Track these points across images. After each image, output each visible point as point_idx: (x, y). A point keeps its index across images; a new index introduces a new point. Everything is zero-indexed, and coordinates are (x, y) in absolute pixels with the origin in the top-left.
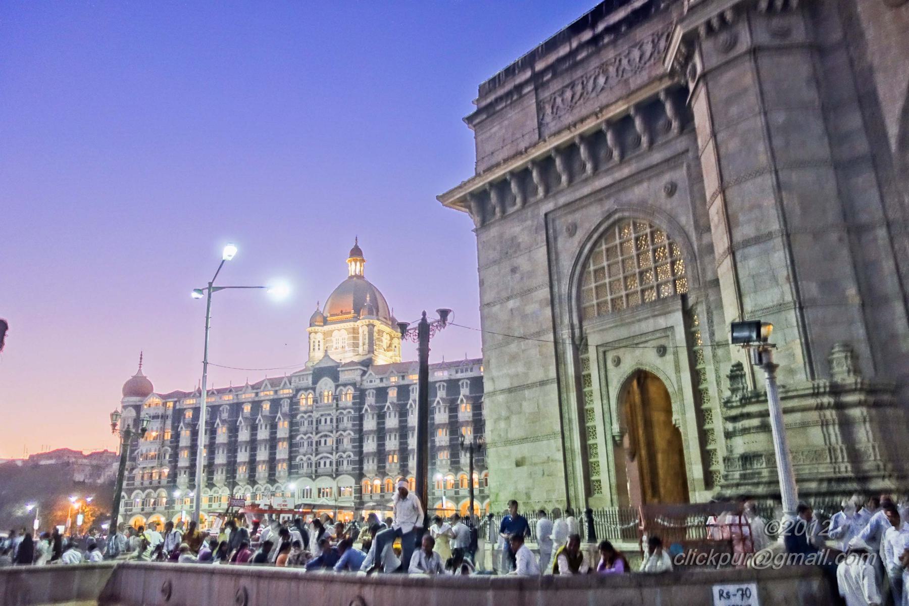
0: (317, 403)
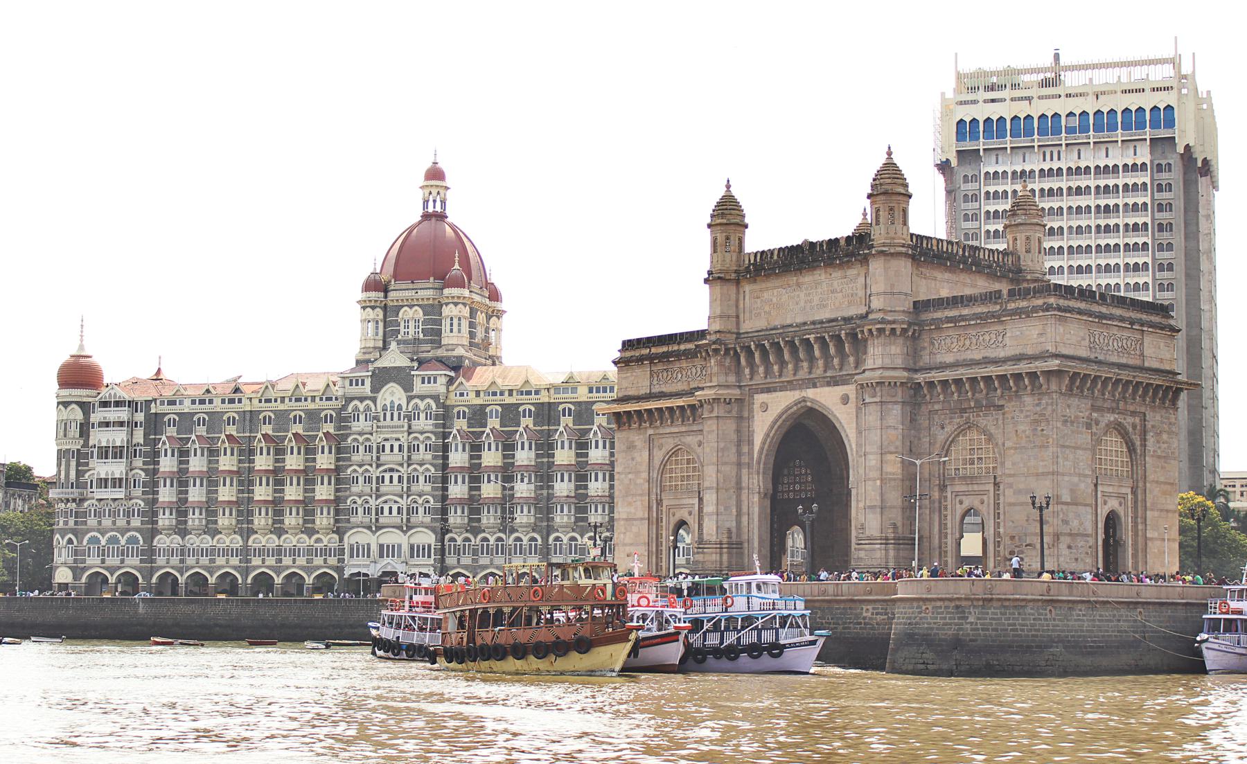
0: (379, 421)
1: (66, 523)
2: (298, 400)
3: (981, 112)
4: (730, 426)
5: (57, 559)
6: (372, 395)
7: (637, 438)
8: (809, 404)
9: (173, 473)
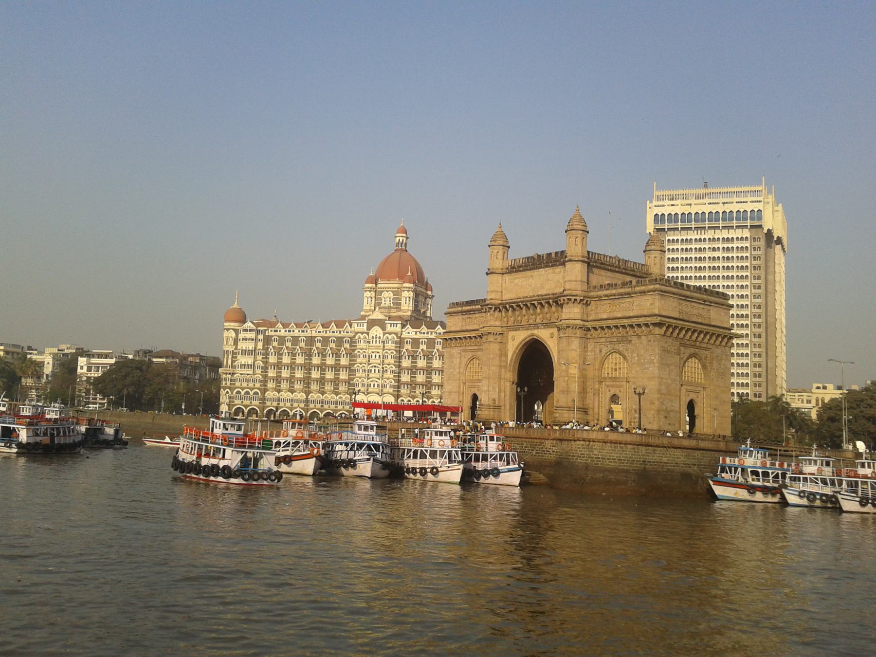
0: (370, 343)
1: (226, 384)
2: (333, 332)
3: (666, 211)
4: (495, 347)
6: (366, 331)
8: (535, 337)
9: (275, 363)
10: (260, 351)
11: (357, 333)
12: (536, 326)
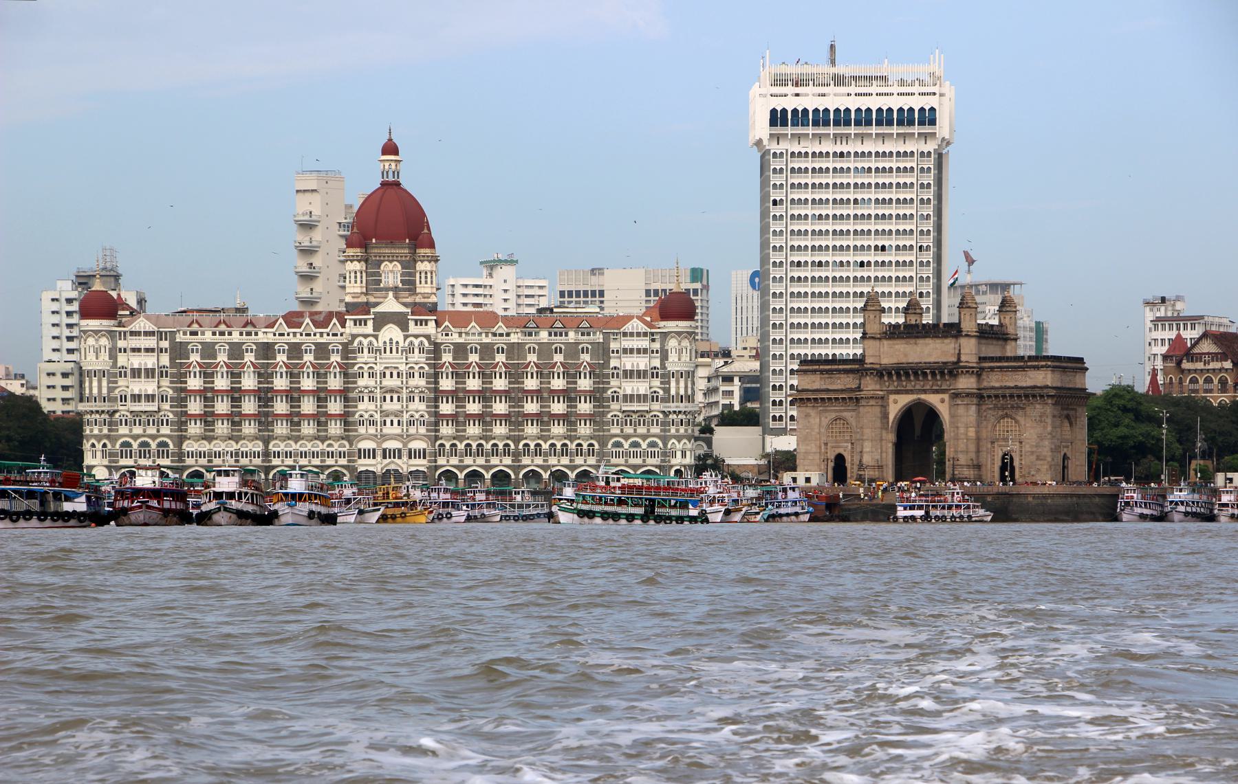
1: (91, 431)
2: (308, 335)
5: (88, 460)
7: (812, 412)
10: (164, 370)
11: (354, 337)
12: (925, 392)
